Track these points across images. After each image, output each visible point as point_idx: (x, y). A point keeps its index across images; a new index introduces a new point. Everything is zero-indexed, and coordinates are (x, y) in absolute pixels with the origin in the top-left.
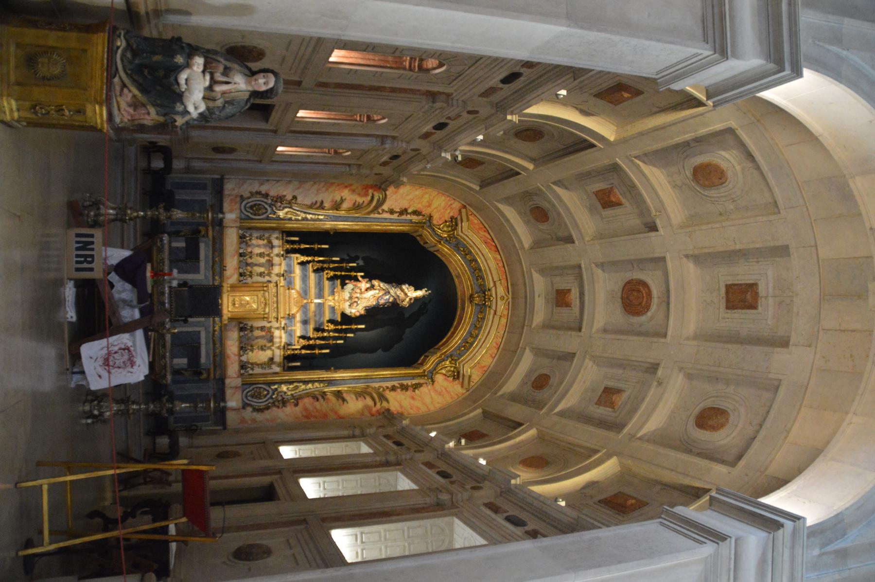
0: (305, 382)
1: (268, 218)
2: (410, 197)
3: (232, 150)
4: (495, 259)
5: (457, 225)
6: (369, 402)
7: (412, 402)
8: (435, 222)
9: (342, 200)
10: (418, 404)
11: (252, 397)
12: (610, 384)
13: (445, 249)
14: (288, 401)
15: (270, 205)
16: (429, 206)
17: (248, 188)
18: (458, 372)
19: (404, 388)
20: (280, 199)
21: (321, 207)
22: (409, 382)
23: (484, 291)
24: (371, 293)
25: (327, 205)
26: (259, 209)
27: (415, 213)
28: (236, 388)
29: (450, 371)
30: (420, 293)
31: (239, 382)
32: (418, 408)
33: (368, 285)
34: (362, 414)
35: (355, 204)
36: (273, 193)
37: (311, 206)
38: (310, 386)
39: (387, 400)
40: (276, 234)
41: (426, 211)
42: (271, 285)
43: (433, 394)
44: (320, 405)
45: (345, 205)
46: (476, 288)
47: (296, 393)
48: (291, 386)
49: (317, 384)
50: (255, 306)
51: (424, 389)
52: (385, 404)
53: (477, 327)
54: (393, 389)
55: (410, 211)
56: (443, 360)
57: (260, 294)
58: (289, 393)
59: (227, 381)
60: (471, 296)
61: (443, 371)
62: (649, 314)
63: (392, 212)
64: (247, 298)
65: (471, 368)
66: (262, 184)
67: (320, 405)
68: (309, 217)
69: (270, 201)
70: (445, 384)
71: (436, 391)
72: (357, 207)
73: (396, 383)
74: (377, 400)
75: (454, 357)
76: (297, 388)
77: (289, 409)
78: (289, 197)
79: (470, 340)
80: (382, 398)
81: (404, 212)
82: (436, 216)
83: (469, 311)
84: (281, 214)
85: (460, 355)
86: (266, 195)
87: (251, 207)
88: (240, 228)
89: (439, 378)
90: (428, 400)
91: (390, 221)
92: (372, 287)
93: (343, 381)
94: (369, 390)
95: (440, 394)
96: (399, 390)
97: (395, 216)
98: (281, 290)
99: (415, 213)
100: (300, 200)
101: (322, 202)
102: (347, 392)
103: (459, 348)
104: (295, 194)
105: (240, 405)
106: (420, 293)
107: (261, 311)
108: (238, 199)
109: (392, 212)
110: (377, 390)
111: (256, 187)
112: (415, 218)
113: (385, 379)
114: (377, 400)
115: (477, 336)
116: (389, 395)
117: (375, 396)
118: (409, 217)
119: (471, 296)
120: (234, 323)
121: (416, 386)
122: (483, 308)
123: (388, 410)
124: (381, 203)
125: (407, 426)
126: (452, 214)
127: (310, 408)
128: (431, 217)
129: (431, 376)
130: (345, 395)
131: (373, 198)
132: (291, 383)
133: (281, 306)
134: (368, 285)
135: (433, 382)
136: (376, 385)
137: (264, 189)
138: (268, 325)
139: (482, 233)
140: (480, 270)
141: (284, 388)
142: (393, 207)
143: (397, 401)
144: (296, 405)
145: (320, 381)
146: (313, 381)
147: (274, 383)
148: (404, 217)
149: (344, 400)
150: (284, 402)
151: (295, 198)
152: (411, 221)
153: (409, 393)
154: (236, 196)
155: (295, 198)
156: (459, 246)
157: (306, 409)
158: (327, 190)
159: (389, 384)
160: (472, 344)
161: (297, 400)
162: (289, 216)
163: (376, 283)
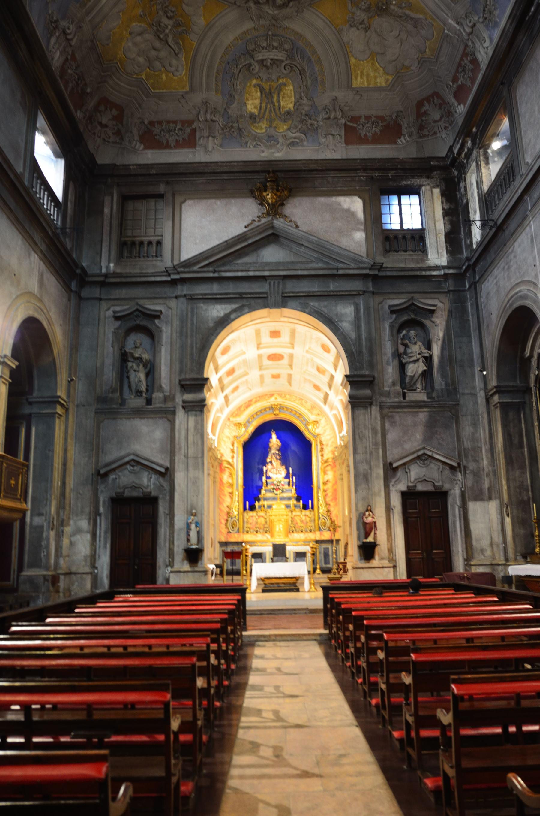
0: (318, 500)
1: (238, 520)
2: (225, 447)
3: (212, 539)
4: (256, 402)
5: (239, 423)
6: (329, 468)
7: (329, 445)
8: (237, 434)
9: (228, 483)
10: (330, 443)
11: (325, 526)
12: (315, 368)
13: (251, 429)
14: (328, 509)
15: (232, 518)
16: (229, 438)
17: (224, 531)
18: (315, 421)
19: (322, 450)
20: (228, 514)
21: (231, 493)
22: (319, 447)
23: (272, 408)
24: (273, 462)
25: (230, 490)
26: (234, 524)
27: (233, 445)
28: (321, 534)
29: (314, 427)
30: (274, 436)
31: (318, 533)
32: (333, 442)
33: (270, 464)
34: (335, 472)
35: (230, 476)
36: (226, 517)
37: (232, 498)
38: (320, 498)
39: (328, 459)
40: (245, 514)
41: (232, 439)
42: (271, 518)
43: (325, 434)
44: (330, 493)
45: (230, 481)
46: (271, 411)
47: (324, 505)
48: (320, 507)
49: (320, 495)
50: (281, 526)
51: (323, 439)
52: (330, 460)
53: (291, 411)
54: (322, 455)
55: (232, 448)
56: (308, 429)
57: (275, 523)
58: (324, 508)
59: (318, 539)
60: (275, 414)
61: (314, 430)
62: (283, 354)
63: (233, 457)
64: (277, 529)
65: (312, 413)
66: (221, 523)
67: (330, 493)
68: (237, 499)
69: (230, 519)
70: (320, 428)
71: (324, 433)
72: (231, 475)
73: (320, 454)
74: (328, 464)
75: (307, 424)
76: (321, 505)
77: (332, 509)
78: (227, 509)
79: (298, 415)
80: (326, 461)
81: (233, 451)
82: (234, 434)
83: (284, 416)
84: (236, 513)
85: (305, 420)
86: (227, 520)
87: (233, 528)
88: (243, 532)
89: (318, 431)
90: (328, 437)
91: (237, 458)
92: (271, 462)
93: (318, 481)
94: (323, 468)
95: (325, 431)
96: (323, 453)
97: (235, 455)
98: (273, 513)
99: (233, 445)
100: (228, 504)
101: (230, 493)
102: (324, 479)
103: (301, 421)
104: (225, 505)
105: (329, 533)
106: (274, 436)
107: (283, 523)
108: (229, 534)
109: (233, 457)
110: (323, 464)
111: (223, 526)
112: (236, 445)
113: (318, 461)
114: (328, 464)
115: (296, 411)
116: (325, 457)
117: (326, 465)
118: (235, 448)
119: (275, 414)
120: (289, 536)
121: (321, 443)
122: (281, 408)
123: (333, 458)
124: (229, 463)
125: (344, 443)
126: (233, 425)
127: (331, 498)
128: (236, 437)
129: (316, 436)
130: (325, 480)
131: (226, 467)
132: (318, 507)
133: (281, 513)
134: (270, 464)
135: (318, 435)
136: (320, 464)
137: (224, 522)
138: (290, 519)
139: (242, 409)
140: (262, 410)
141: (321, 511)
142: (230, 457)
143: (328, 455)
144: (330, 505)
145: (318, 493)
146: (318, 496)
147: (319, 516)
148: (235, 451)
149: (328, 481)
150: (328, 511)
151: (228, 507)
152: (237, 447)
153: (324, 447)
154: (227, 535)
155: (228, 507)
156: (249, 422)
157: (332, 500)
158: (223, 490)
159: (320, 457)
160: (300, 414)
161: (327, 504)
162: (237, 509)
163: (268, 460)
